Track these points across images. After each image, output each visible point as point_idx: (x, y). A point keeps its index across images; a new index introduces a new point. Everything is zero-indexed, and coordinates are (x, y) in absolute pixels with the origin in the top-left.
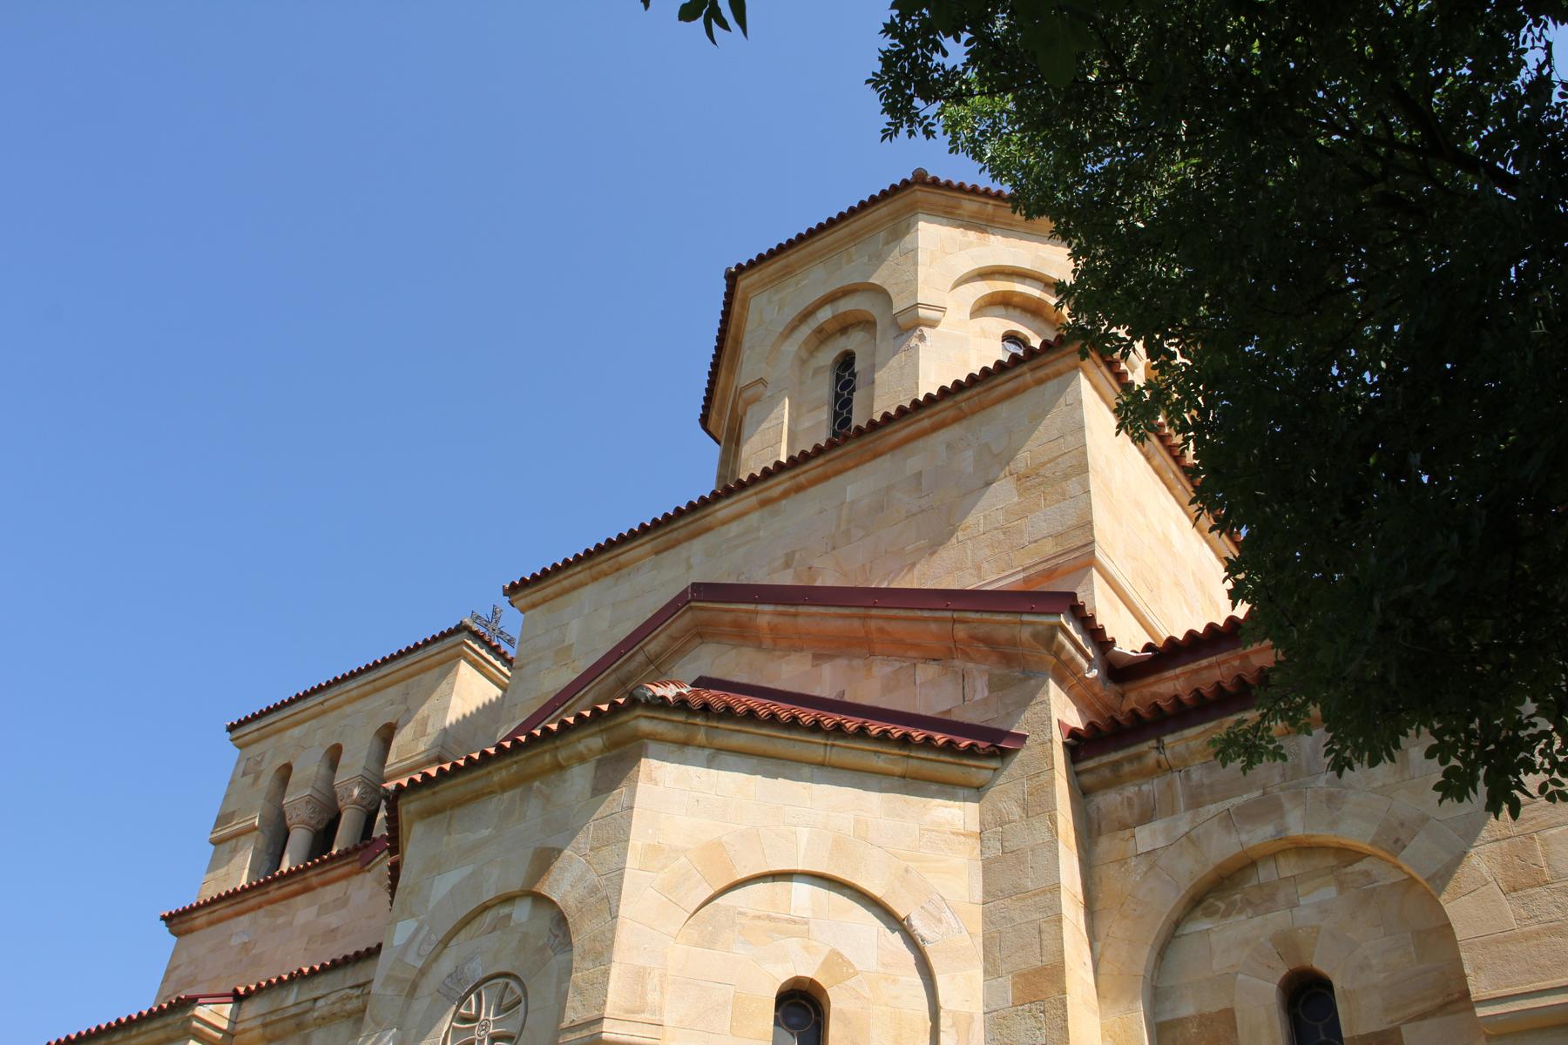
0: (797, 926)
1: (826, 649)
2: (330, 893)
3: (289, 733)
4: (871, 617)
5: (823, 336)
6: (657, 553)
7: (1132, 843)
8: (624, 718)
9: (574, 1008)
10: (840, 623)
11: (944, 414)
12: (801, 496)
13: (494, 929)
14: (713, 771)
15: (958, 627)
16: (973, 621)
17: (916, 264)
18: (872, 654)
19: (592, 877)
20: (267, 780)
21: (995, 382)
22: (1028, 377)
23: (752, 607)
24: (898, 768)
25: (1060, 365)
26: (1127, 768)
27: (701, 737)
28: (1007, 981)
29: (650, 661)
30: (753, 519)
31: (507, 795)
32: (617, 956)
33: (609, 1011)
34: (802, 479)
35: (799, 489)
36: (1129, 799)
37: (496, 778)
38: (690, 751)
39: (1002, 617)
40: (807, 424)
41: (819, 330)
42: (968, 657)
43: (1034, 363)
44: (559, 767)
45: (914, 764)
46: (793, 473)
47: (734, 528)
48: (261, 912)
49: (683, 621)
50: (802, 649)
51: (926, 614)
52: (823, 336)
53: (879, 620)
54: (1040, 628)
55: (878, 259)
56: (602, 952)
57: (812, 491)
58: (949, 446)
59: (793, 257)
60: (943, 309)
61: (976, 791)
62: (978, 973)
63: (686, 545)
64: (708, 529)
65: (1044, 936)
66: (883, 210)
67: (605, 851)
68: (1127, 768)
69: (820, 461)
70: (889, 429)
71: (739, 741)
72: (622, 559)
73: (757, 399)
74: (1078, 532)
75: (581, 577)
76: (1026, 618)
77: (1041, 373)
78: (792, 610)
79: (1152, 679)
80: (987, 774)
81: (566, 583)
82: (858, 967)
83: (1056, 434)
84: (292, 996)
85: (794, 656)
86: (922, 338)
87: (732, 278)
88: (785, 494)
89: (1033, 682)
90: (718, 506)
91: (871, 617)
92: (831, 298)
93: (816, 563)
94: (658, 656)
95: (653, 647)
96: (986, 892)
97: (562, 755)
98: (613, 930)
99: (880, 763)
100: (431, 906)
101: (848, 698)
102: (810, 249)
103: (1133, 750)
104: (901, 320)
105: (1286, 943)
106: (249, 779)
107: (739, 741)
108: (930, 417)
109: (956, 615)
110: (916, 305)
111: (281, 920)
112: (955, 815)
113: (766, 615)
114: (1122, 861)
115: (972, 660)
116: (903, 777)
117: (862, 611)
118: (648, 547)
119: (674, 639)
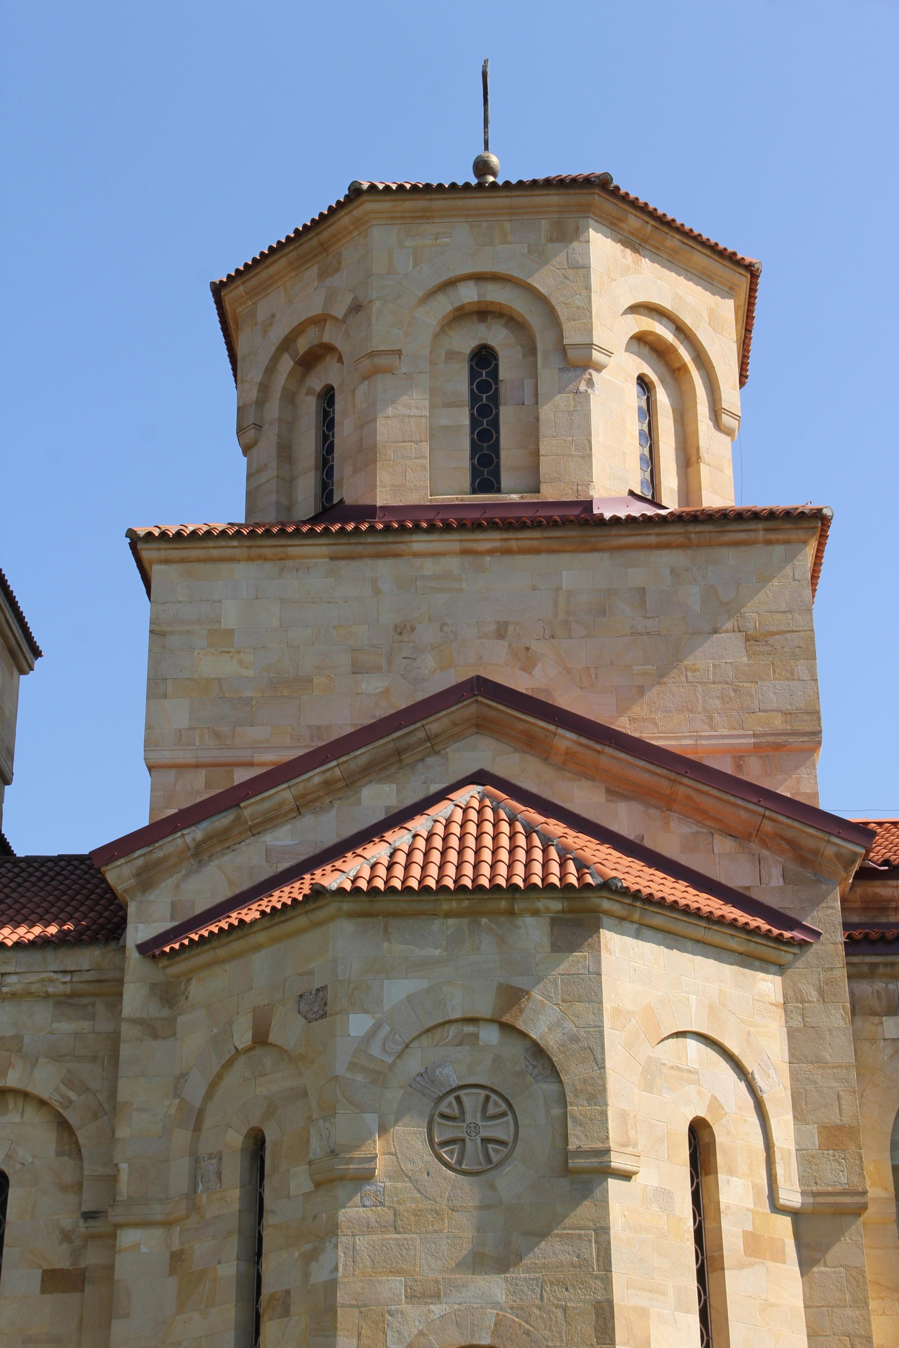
0: (691, 1075)
1: (620, 790)
4: (681, 783)
6: (332, 558)
7: (880, 1028)
8: (590, 895)
9: (577, 1137)
10: (647, 776)
11: (671, 538)
12: (508, 560)
13: (460, 1044)
14: (640, 942)
15: (765, 821)
16: (782, 823)
17: (588, 288)
18: (669, 810)
19: (569, 1026)
21: (728, 528)
22: (761, 535)
23: (552, 728)
24: (741, 949)
25: (793, 536)
26: (882, 970)
27: (636, 916)
28: (813, 1129)
29: (429, 739)
30: (453, 564)
31: (451, 922)
32: (611, 1100)
33: (613, 1145)
34: (514, 544)
35: (507, 552)
36: (878, 993)
37: (446, 906)
38: (626, 924)
39: (812, 831)
40: (444, 422)
41: (460, 309)
42: (764, 843)
43: (770, 524)
44: (511, 913)
45: (752, 946)
46: (505, 535)
47: (430, 567)
49: (466, 710)
50: (593, 779)
51: (739, 802)
53: (686, 787)
54: (843, 851)
55: (541, 257)
56: (597, 1093)
57: (520, 559)
58: (673, 572)
59: (438, 203)
60: (609, 354)
61: (781, 968)
62: (790, 1117)
63: (369, 562)
64: (397, 555)
65: (843, 1102)
66: (553, 198)
67: (579, 1007)
68: (882, 970)
69: (537, 534)
70: (615, 531)
71: (658, 921)
72: (291, 551)
73: (389, 370)
74: (806, 717)
75: (237, 552)
76: (834, 839)
77: (773, 536)
78: (598, 747)
79: (878, 883)
80: (790, 957)
81: (215, 553)
82: (727, 1110)
83: (783, 607)
85: (584, 783)
86: (590, 383)
87: (355, 192)
88: (491, 552)
89: (824, 887)
90: (415, 538)
91: (681, 783)
92: (479, 278)
93: (535, 646)
94: (437, 736)
95: (435, 724)
96: (792, 1055)
97: (519, 906)
98: (603, 1078)
99: (733, 944)
100: (386, 1008)
101: (648, 843)
102: (460, 203)
103: (890, 959)
104: (570, 353)
107: (658, 921)
108: (658, 535)
109: (767, 813)
110: (590, 345)
112: (768, 985)
113: (566, 739)
114: (873, 1040)
115: (768, 849)
116: (741, 954)
117: (673, 776)
118: (324, 550)
119: (455, 725)
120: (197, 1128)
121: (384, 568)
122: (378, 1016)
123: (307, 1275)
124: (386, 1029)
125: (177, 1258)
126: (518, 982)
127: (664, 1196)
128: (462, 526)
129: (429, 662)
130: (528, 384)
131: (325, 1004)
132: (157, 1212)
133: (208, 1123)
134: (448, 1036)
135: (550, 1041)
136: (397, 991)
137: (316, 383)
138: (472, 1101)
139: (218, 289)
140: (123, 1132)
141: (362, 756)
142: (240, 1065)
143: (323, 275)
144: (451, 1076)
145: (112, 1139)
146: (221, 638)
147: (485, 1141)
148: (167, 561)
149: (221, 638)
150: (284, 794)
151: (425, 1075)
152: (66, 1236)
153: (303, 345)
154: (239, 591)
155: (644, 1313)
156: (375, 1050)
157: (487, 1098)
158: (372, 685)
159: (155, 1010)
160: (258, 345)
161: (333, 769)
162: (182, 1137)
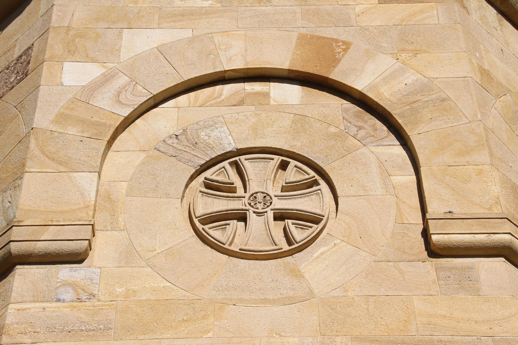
13: (241, 103)
122: (111, 65)
124: (123, 80)
126: (329, 32)
131: (29, 63)
134: (221, 95)
147: (280, 216)
151: (182, 138)
156: (104, 101)
157: (284, 166)
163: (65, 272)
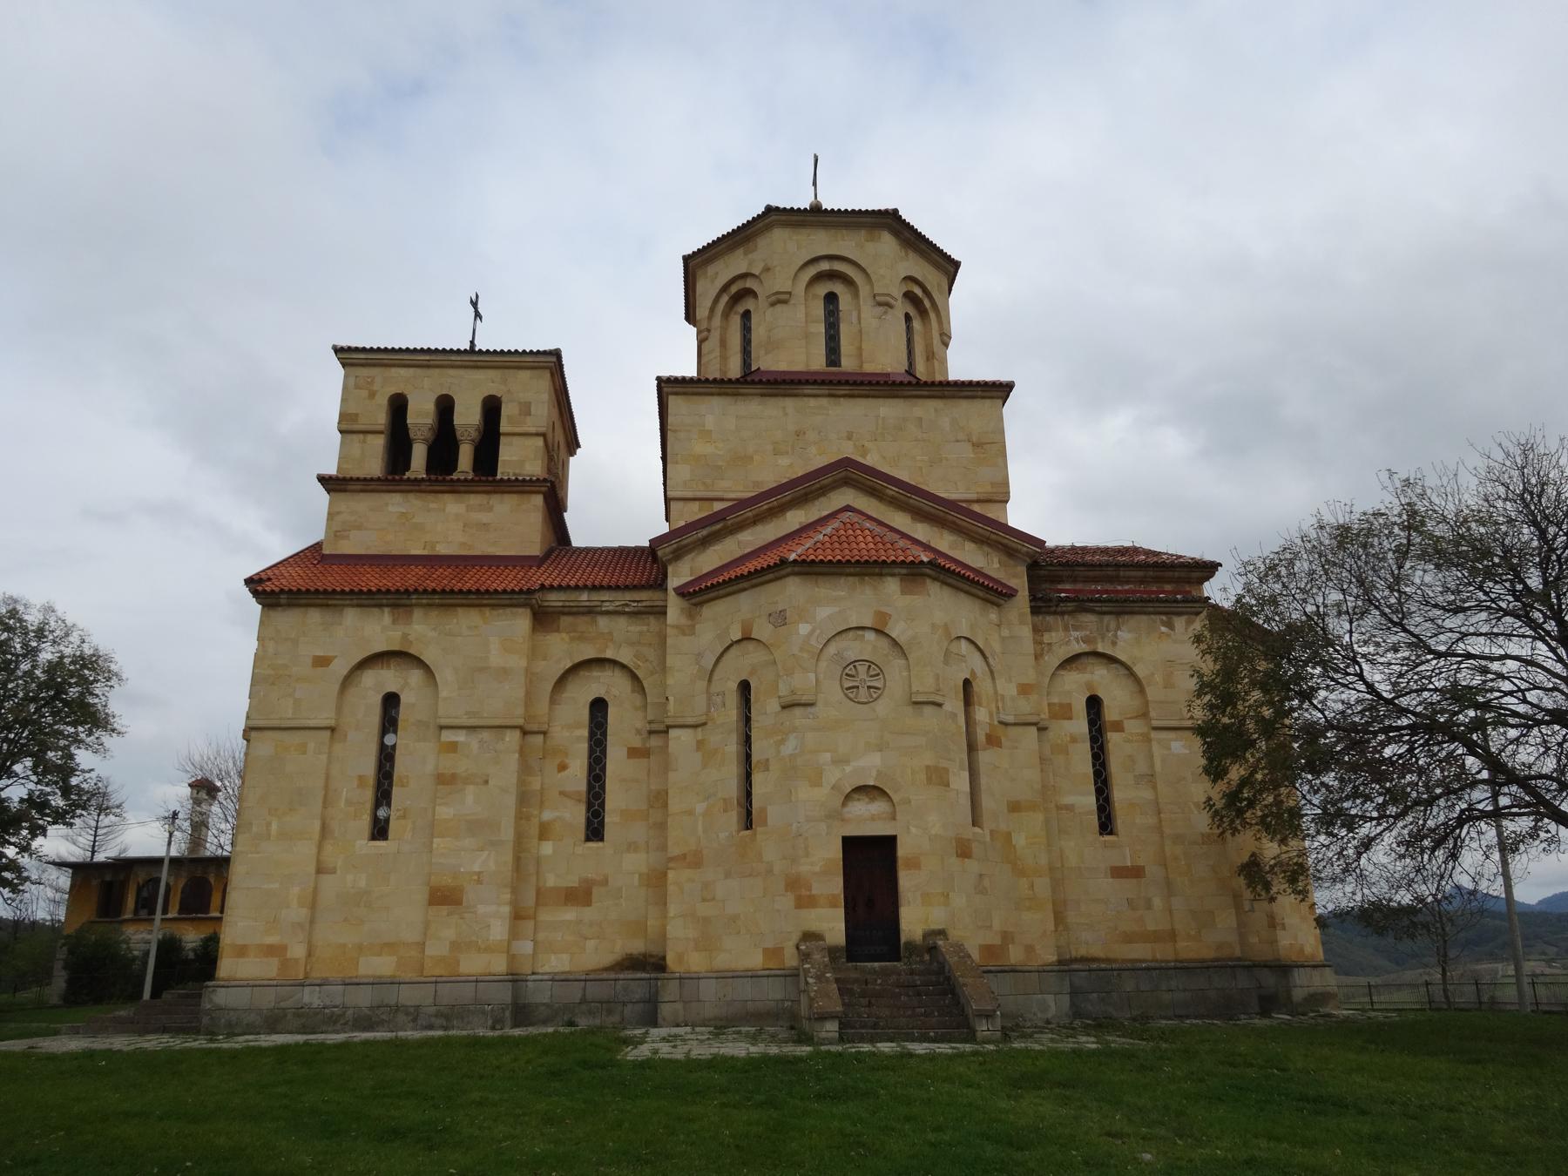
2: (474, 499)
3: (393, 370)
5: (820, 277)
20: (382, 401)
42: (989, 545)
44: (881, 575)
47: (812, 402)
48: (411, 496)
52: (820, 277)
61: (998, 605)
84: (584, 596)
87: (769, 210)
88: (844, 396)
97: (885, 571)
99: (981, 594)
105: (1089, 685)
106: (365, 393)
107: (950, 581)
111: (432, 506)
113: (892, 490)
120: (710, 680)
121: (789, 403)
123: (779, 752)
125: (700, 744)
126: (884, 609)
127: (954, 716)
128: (831, 383)
129: (813, 450)
130: (855, 314)
132: (690, 721)
133: (715, 677)
135: (902, 640)
136: (823, 612)
137: (741, 309)
138: (862, 669)
139: (686, 259)
140: (670, 681)
141: (788, 496)
142: (733, 651)
143: (746, 254)
144: (852, 655)
145: (664, 685)
146: (706, 435)
148: (676, 394)
149: (706, 435)
150: (748, 513)
152: (638, 732)
153: (734, 289)
154: (714, 412)
155: (946, 770)
156: (813, 642)
158: (784, 461)
159: (684, 621)
160: (708, 289)
161: (774, 502)
162: (701, 685)
163: (809, 709)
